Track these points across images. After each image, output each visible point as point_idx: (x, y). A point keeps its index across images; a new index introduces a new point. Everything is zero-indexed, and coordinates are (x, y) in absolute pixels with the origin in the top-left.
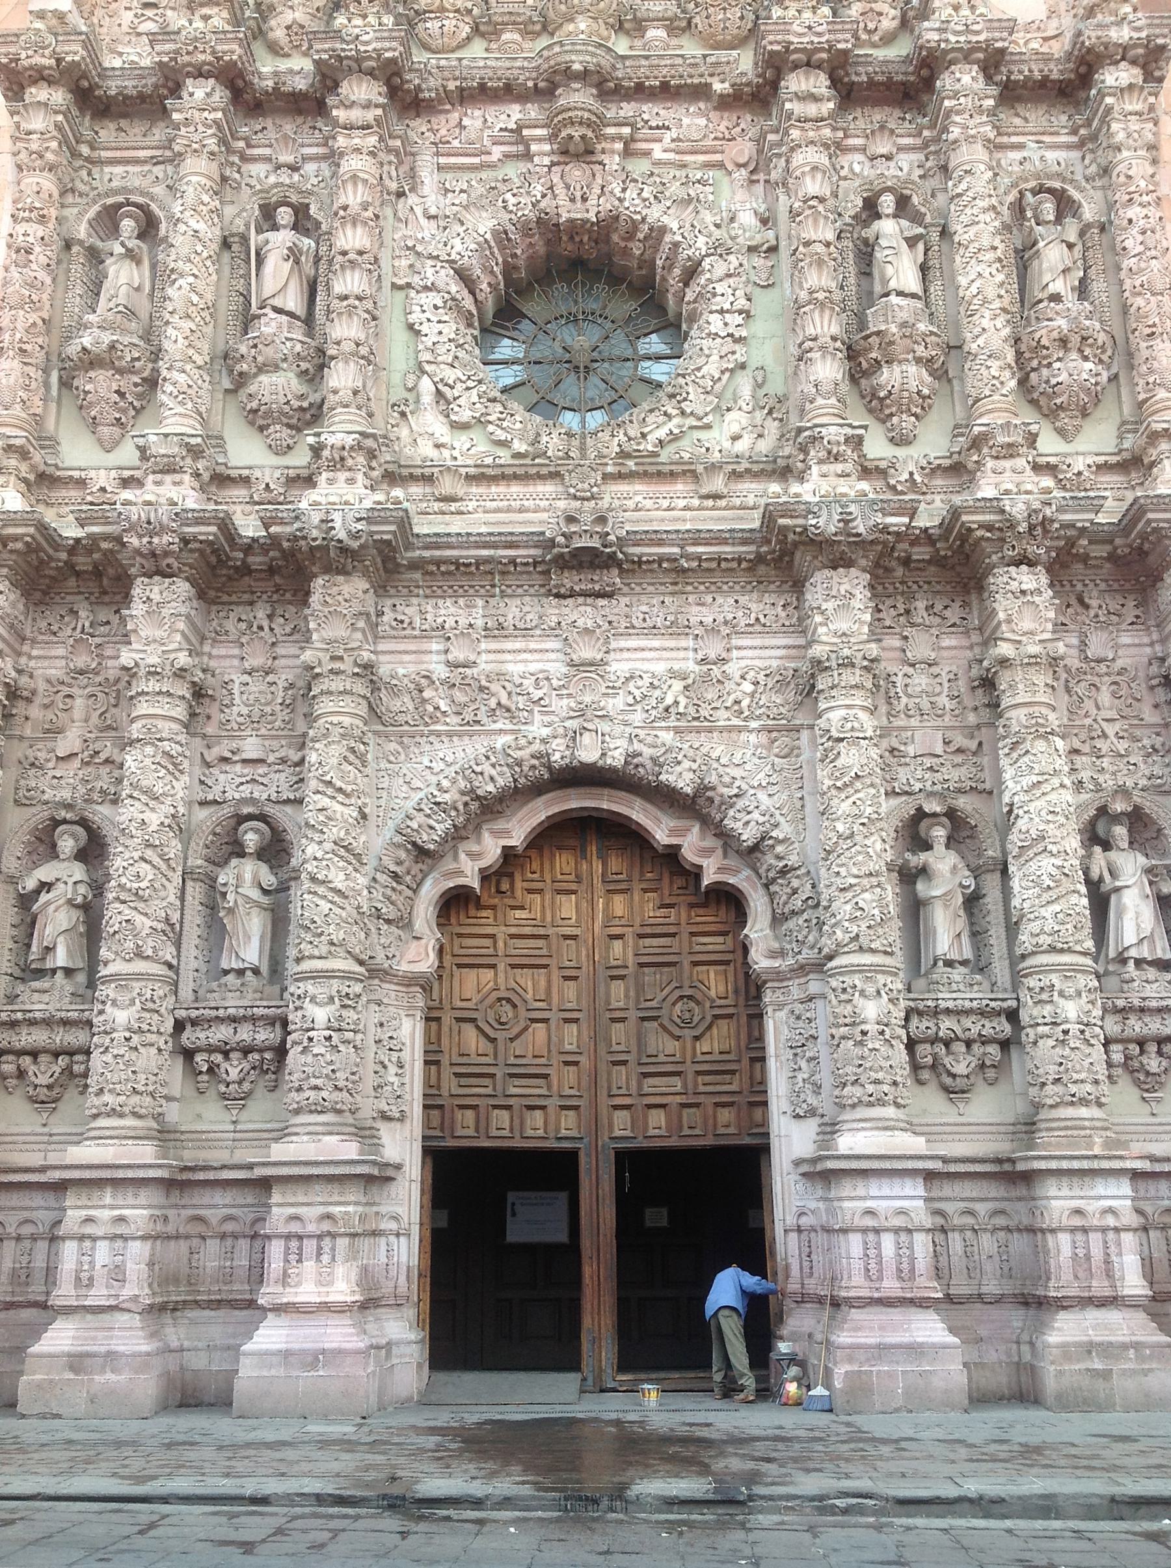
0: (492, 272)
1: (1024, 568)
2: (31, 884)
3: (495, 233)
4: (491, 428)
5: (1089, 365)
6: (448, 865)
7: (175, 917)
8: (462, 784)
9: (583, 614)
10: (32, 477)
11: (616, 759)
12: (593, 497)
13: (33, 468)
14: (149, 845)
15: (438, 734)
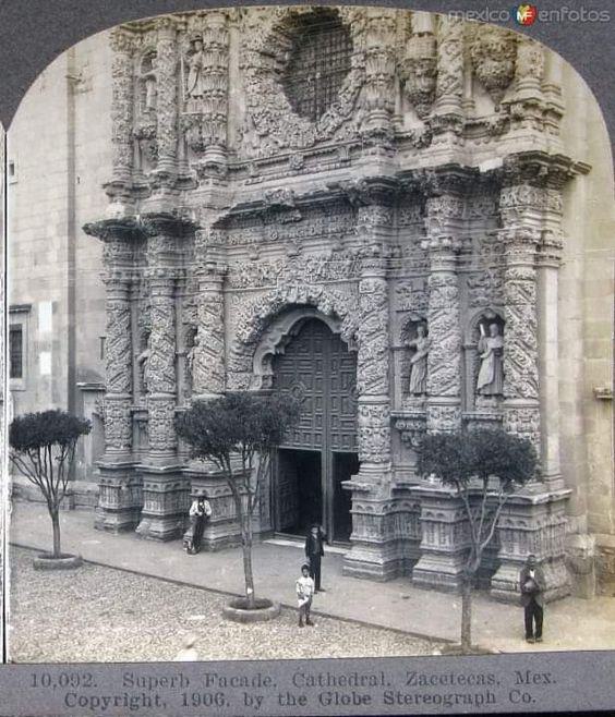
0: (280, 45)
1: (436, 199)
2: (140, 358)
3: (274, 29)
4: (271, 136)
5: (496, 64)
6: (264, 345)
7: (171, 373)
8: (254, 314)
9: (292, 232)
10: (128, 193)
11: (303, 300)
12: (302, 168)
13: (127, 189)
14: (156, 348)
15: (249, 291)
